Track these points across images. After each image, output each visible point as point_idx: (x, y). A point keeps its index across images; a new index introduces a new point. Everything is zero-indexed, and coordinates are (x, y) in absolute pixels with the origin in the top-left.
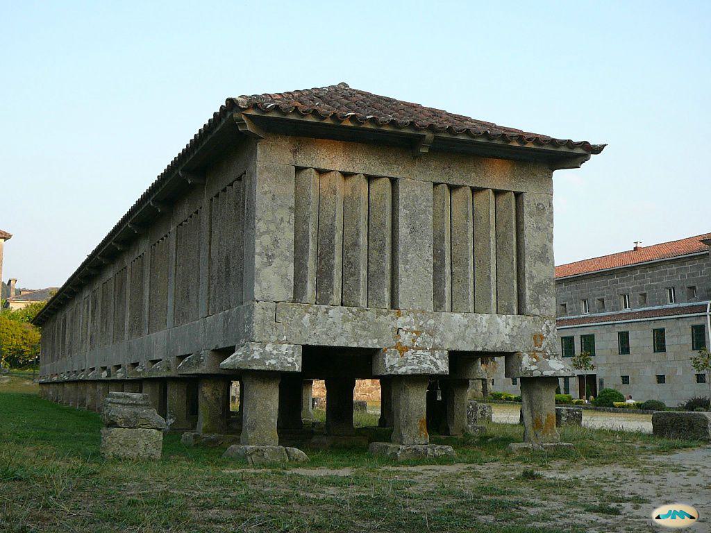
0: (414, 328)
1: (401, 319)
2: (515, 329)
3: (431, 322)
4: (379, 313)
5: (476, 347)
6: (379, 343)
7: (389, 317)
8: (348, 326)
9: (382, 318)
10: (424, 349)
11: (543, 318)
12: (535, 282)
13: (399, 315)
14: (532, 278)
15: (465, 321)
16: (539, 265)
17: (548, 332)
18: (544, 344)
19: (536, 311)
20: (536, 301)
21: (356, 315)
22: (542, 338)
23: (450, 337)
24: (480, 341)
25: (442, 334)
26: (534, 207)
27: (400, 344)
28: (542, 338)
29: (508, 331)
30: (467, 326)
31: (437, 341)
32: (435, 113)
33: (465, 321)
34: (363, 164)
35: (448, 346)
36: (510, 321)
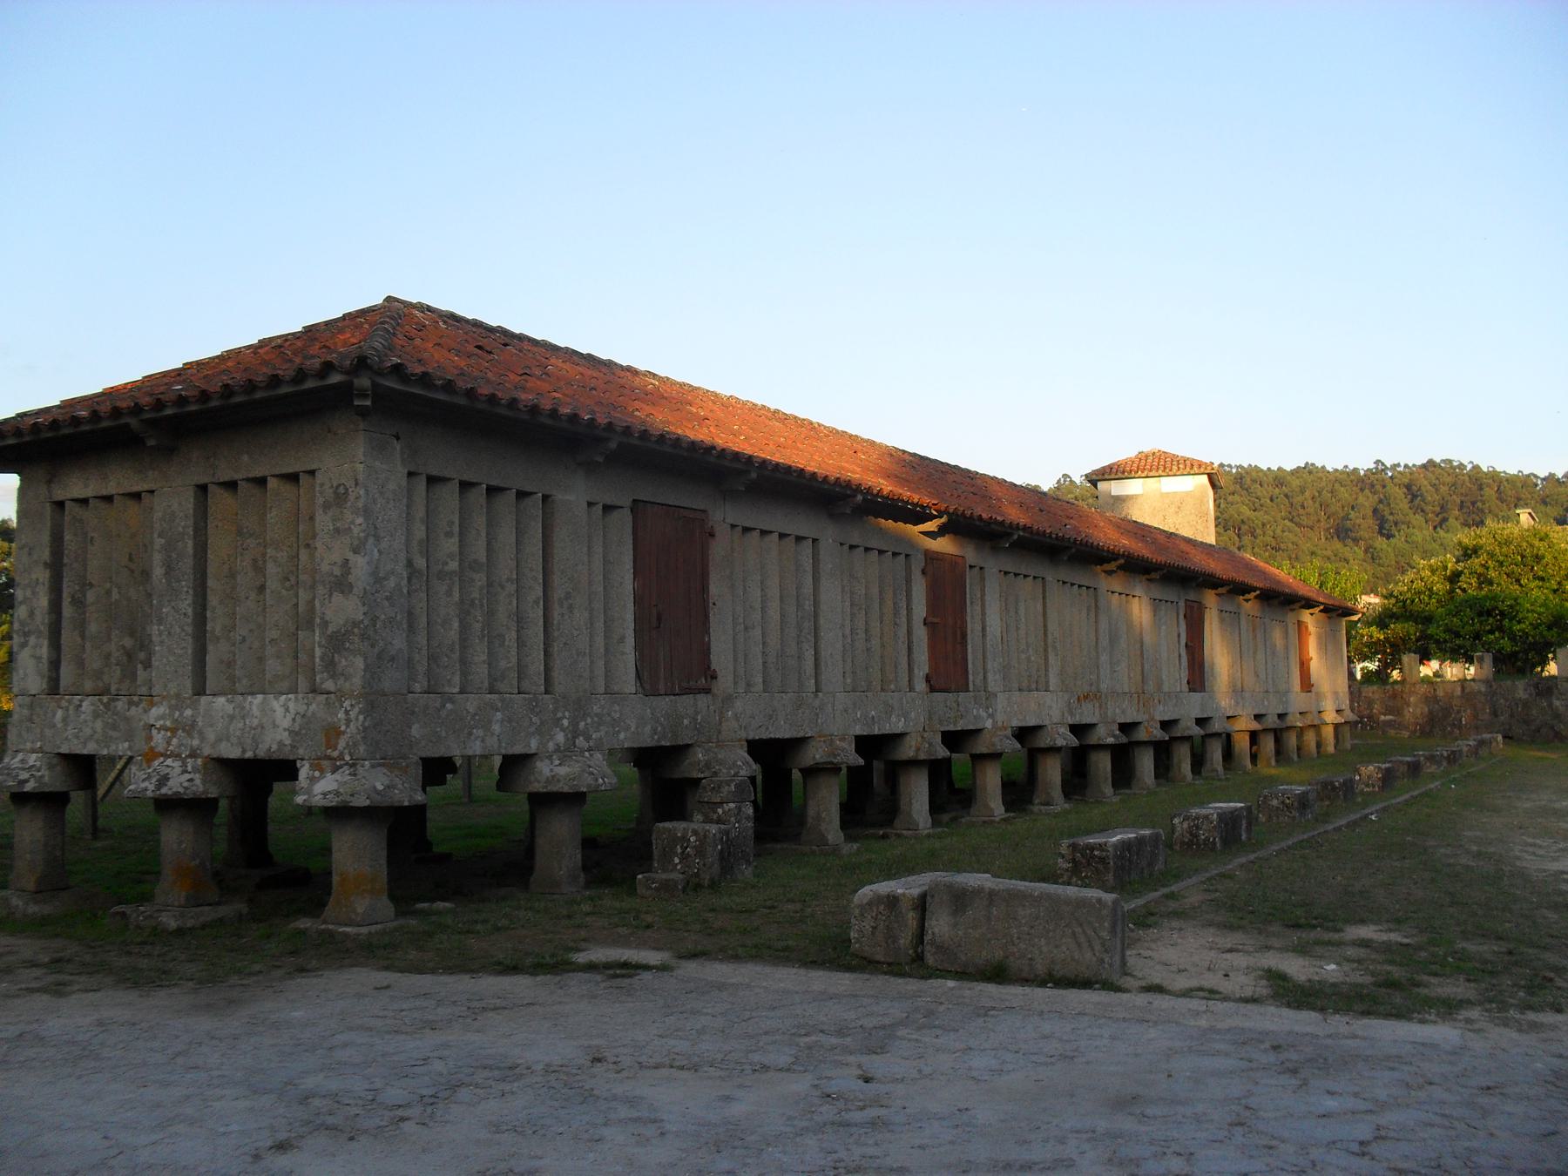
0: (168, 723)
1: (154, 711)
2: (298, 719)
3: (188, 712)
4: (131, 703)
5: (244, 751)
6: (130, 748)
7: (140, 709)
8: (99, 725)
9: (133, 711)
10: (177, 756)
11: (341, 695)
12: (330, 630)
13: (152, 704)
14: (325, 624)
15: (229, 708)
16: (337, 598)
17: (348, 721)
18: (342, 744)
19: (329, 685)
20: (330, 665)
21: (107, 706)
22: (340, 733)
23: (211, 736)
24: (249, 741)
25: (201, 733)
26: (329, 492)
27: (152, 749)
28: (340, 733)
29: (286, 723)
30: (232, 718)
31: (196, 742)
32: (109, 394)
33: (229, 708)
34: (118, 479)
35: (207, 751)
36: (291, 705)
